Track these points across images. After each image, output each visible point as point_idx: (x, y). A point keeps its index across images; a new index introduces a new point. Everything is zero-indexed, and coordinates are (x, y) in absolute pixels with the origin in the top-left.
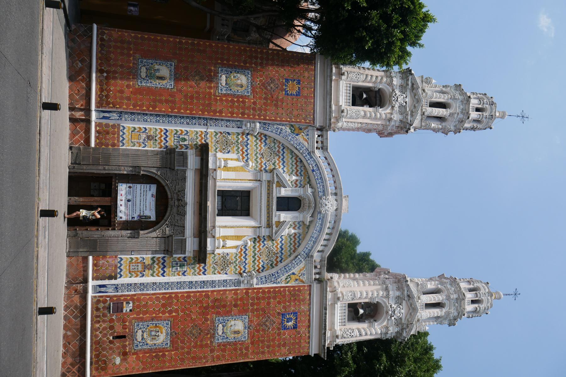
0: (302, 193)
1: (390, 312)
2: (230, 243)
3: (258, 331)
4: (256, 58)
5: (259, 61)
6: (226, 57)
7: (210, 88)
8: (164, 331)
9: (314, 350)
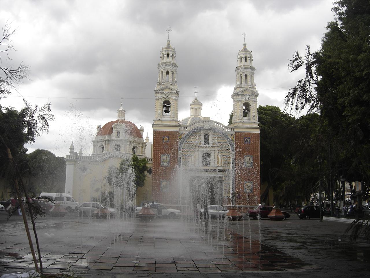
0: (203, 135)
1: (247, 100)
2: (220, 161)
3: (250, 152)
4: (157, 153)
5: (158, 151)
6: (157, 163)
7: (168, 168)
8: (247, 183)
9: (258, 131)
